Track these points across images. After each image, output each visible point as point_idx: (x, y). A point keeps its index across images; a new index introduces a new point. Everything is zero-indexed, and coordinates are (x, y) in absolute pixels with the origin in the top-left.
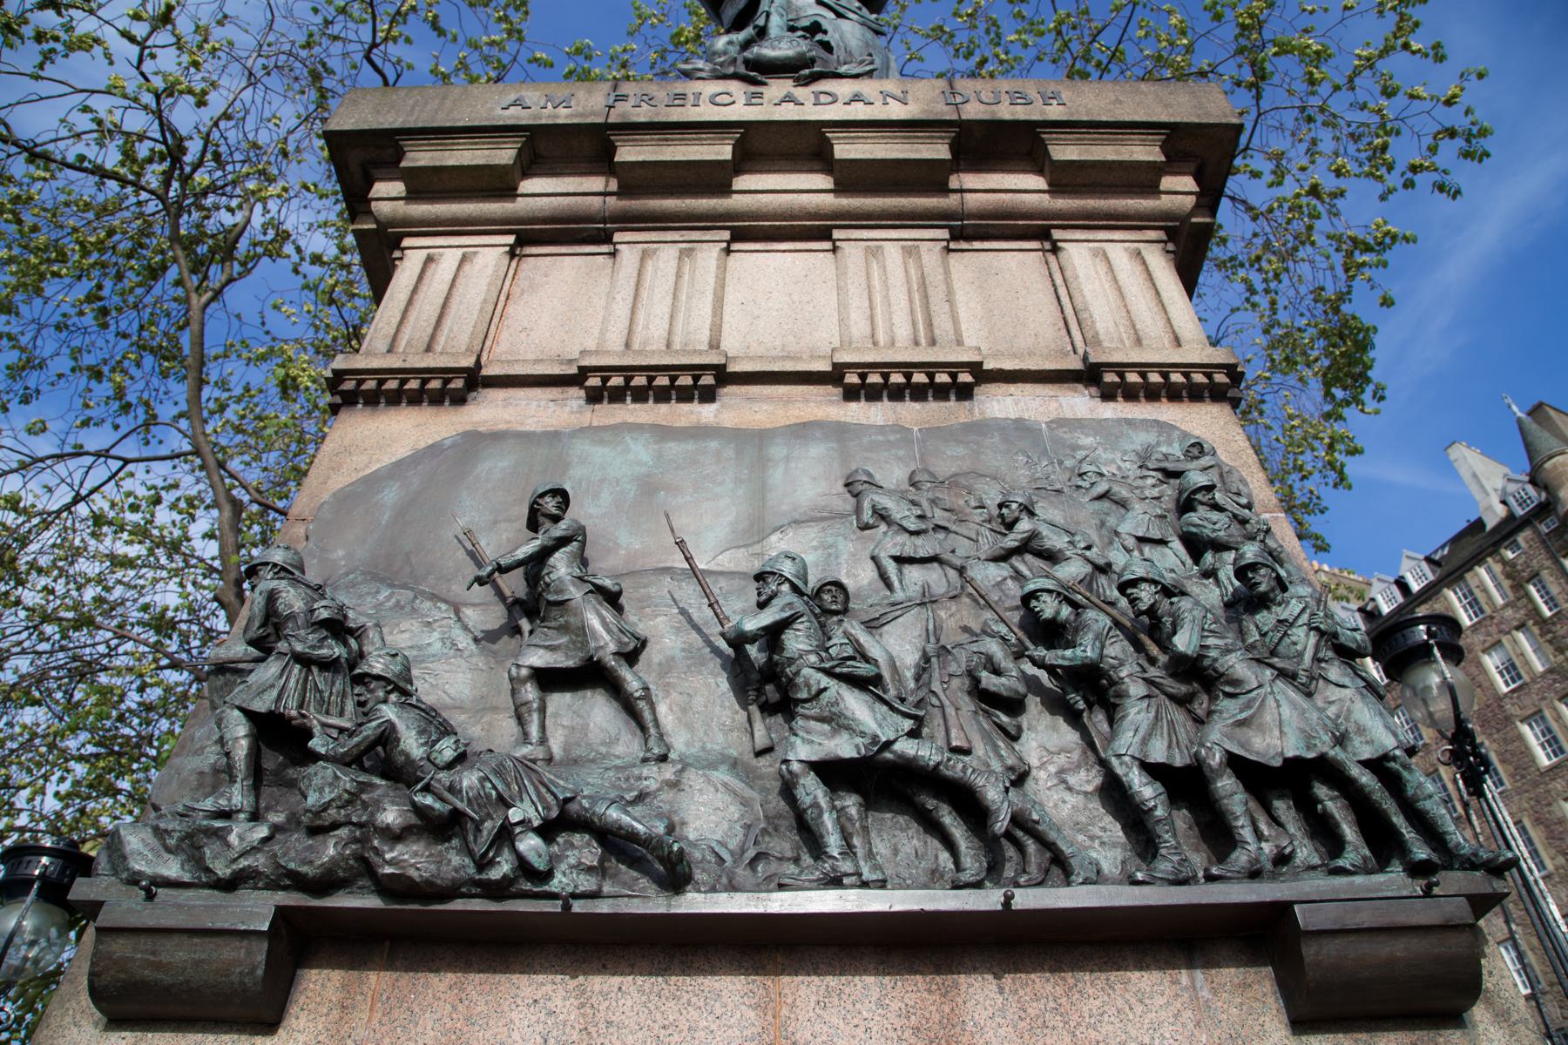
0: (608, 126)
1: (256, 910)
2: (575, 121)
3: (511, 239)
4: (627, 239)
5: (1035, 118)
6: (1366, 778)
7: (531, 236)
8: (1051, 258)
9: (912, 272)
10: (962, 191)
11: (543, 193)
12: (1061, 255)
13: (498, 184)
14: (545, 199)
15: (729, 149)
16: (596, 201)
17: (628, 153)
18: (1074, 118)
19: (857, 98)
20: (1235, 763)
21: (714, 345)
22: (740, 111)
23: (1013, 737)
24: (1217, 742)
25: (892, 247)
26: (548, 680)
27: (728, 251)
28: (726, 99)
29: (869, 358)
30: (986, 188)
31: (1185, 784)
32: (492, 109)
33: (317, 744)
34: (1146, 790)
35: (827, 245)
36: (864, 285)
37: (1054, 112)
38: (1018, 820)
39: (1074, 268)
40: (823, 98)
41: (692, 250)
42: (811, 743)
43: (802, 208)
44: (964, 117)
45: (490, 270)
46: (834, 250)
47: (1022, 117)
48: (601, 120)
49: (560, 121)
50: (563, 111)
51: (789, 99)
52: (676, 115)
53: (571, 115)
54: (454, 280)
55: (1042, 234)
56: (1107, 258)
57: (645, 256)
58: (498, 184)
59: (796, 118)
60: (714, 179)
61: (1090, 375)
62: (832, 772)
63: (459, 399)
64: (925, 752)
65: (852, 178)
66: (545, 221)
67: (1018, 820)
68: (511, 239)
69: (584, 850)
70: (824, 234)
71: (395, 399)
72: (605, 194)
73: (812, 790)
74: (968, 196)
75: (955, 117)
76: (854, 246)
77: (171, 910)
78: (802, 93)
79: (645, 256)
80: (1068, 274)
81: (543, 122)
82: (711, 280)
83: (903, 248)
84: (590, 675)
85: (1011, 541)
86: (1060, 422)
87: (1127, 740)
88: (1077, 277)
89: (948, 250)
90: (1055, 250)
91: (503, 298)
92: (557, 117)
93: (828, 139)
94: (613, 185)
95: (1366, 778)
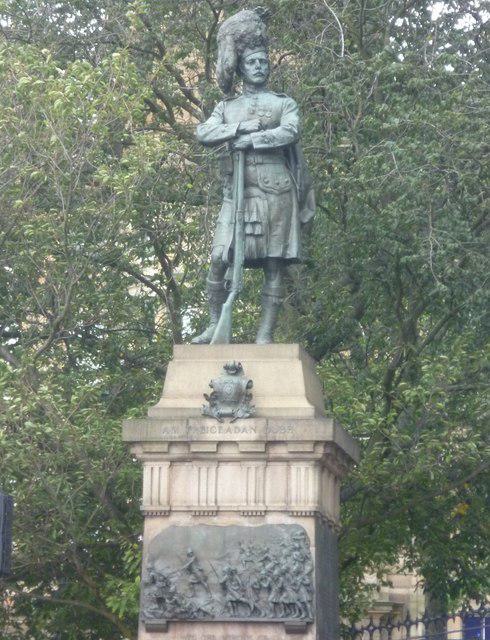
1: (163, 621)
6: (300, 605)
11: (176, 452)
17: (194, 448)
19: (244, 430)
21: (216, 502)
23: (257, 594)
24: (282, 599)
25: (253, 465)
26: (193, 584)
29: (245, 509)
33: (167, 601)
34: (271, 605)
38: (255, 608)
42: (229, 597)
51: (229, 430)
62: (232, 602)
63: (168, 516)
64: (243, 599)
67: (255, 608)
69: (201, 613)
71: (156, 516)
73: (230, 604)
84: (199, 583)
85: (262, 558)
86: (280, 525)
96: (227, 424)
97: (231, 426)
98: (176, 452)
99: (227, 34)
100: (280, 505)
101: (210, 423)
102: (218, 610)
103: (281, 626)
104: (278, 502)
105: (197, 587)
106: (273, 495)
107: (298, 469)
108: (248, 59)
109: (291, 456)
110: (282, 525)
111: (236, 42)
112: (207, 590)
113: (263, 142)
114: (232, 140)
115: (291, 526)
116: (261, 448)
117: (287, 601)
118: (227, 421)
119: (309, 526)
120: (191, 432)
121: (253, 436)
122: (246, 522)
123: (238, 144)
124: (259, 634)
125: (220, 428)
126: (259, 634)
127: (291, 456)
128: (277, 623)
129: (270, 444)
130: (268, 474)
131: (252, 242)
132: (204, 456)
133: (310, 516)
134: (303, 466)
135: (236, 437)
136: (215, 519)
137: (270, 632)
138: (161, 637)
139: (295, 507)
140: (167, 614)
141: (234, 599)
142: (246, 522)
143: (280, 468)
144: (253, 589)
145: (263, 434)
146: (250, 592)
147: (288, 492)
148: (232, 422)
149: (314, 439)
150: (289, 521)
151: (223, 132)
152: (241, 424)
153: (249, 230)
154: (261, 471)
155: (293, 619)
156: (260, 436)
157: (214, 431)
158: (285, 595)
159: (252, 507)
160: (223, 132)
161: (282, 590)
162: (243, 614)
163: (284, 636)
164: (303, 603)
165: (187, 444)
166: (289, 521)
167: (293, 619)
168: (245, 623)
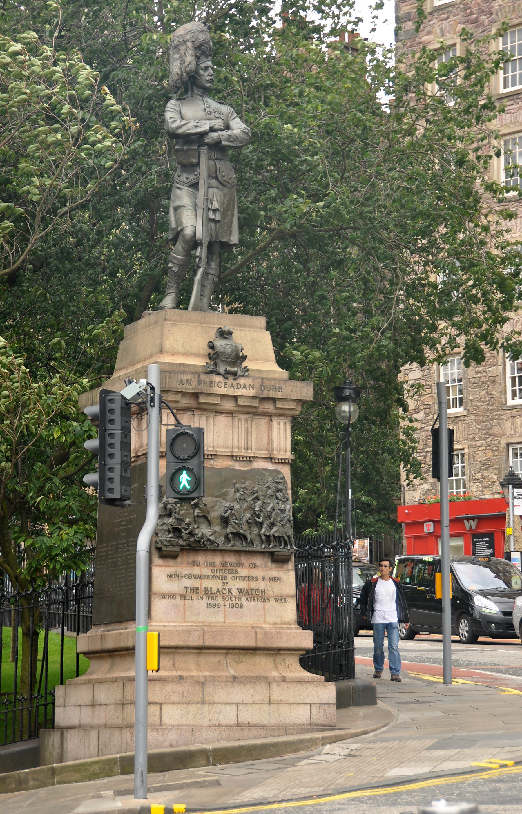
6: (286, 538)
19: (245, 387)
20: (274, 536)
25: (243, 417)
26: (198, 516)
31: (268, 537)
34: (264, 537)
37: (279, 395)
42: (229, 529)
51: (232, 386)
53: (193, 389)
61: (271, 459)
62: (232, 533)
73: (230, 536)
77: (168, 549)
85: (253, 497)
87: (262, 532)
90: (271, 420)
95: (286, 538)
96: (230, 381)
97: (235, 383)
98: (185, 402)
99: (188, 40)
100: (264, 453)
101: (217, 379)
102: (221, 540)
103: (267, 555)
104: (262, 450)
105: (201, 520)
106: (257, 445)
107: (279, 423)
108: (203, 65)
110: (266, 470)
111: (195, 48)
112: (209, 523)
113: (228, 140)
114: (203, 135)
115: (273, 470)
117: (276, 535)
118: (231, 378)
119: (286, 472)
121: (251, 392)
122: (237, 466)
123: (207, 140)
124: (249, 562)
125: (225, 383)
126: (249, 562)
128: (263, 553)
129: (263, 400)
130: (254, 426)
131: (213, 225)
132: (206, 407)
133: (288, 463)
134: (282, 421)
135: (239, 392)
136: (212, 462)
137: (258, 561)
138: (171, 562)
139: (277, 455)
140: (181, 542)
141: (235, 531)
142: (237, 466)
143: (263, 421)
144: (247, 522)
145: (260, 392)
146: (245, 526)
147: (270, 441)
148: (235, 379)
149: (299, 398)
150: (270, 466)
151: (196, 127)
152: (242, 381)
153: (211, 215)
154: (249, 423)
155: (280, 550)
157: (221, 386)
158: (275, 529)
159: (243, 453)
160: (196, 127)
161: (273, 524)
162: (239, 545)
163: (269, 564)
164: (289, 537)
165: (196, 395)
166: (270, 466)
167: (280, 550)
168: (238, 552)
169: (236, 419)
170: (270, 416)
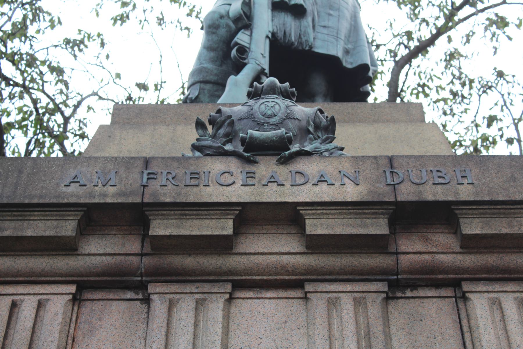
0: (142, 205)
2: (120, 200)
3: (72, 289)
4: (157, 290)
5: (450, 198)
7: (87, 286)
8: (461, 305)
9: (361, 319)
10: (397, 253)
12: (469, 303)
13: (66, 247)
14: (98, 258)
15: (231, 223)
16: (135, 260)
17: (160, 228)
18: (479, 199)
19: (322, 180)
22: (238, 193)
25: (345, 294)
27: (231, 299)
28: (228, 179)
30: (415, 250)
32: (58, 185)
35: (299, 293)
36: (326, 337)
37: (465, 193)
39: (476, 318)
40: (299, 180)
41: (205, 300)
43: (283, 267)
44: (399, 199)
45: (60, 317)
46: (305, 298)
47: (441, 198)
48: (138, 200)
49: (109, 200)
50: (111, 190)
51: (273, 180)
52: (194, 196)
53: (118, 195)
54: (34, 327)
55: (456, 284)
56: (501, 308)
57: (171, 305)
58: (66, 247)
59: (279, 200)
60: (222, 245)
65: (317, 244)
66: (98, 275)
68: (72, 289)
70: (298, 285)
72: (142, 255)
74: (402, 257)
75: (392, 199)
76: (320, 294)
78: (283, 172)
79: (171, 305)
80: (473, 322)
81: (96, 201)
82: (219, 329)
83: (355, 299)
88: (478, 327)
89: (388, 299)
90: (464, 298)
91: (70, 342)
92: (105, 195)
93: (302, 215)
94: (147, 249)
96: (267, 166)
98: (101, 251)
101: (216, 166)
107: (497, 304)
109: (469, 260)
116: (378, 227)
120: (155, 185)
125: (251, 175)
127: (469, 260)
132: (189, 261)
143: (433, 310)
145: (382, 187)
152: (311, 167)
156: (370, 192)
169: (319, 303)
170: (452, 284)
